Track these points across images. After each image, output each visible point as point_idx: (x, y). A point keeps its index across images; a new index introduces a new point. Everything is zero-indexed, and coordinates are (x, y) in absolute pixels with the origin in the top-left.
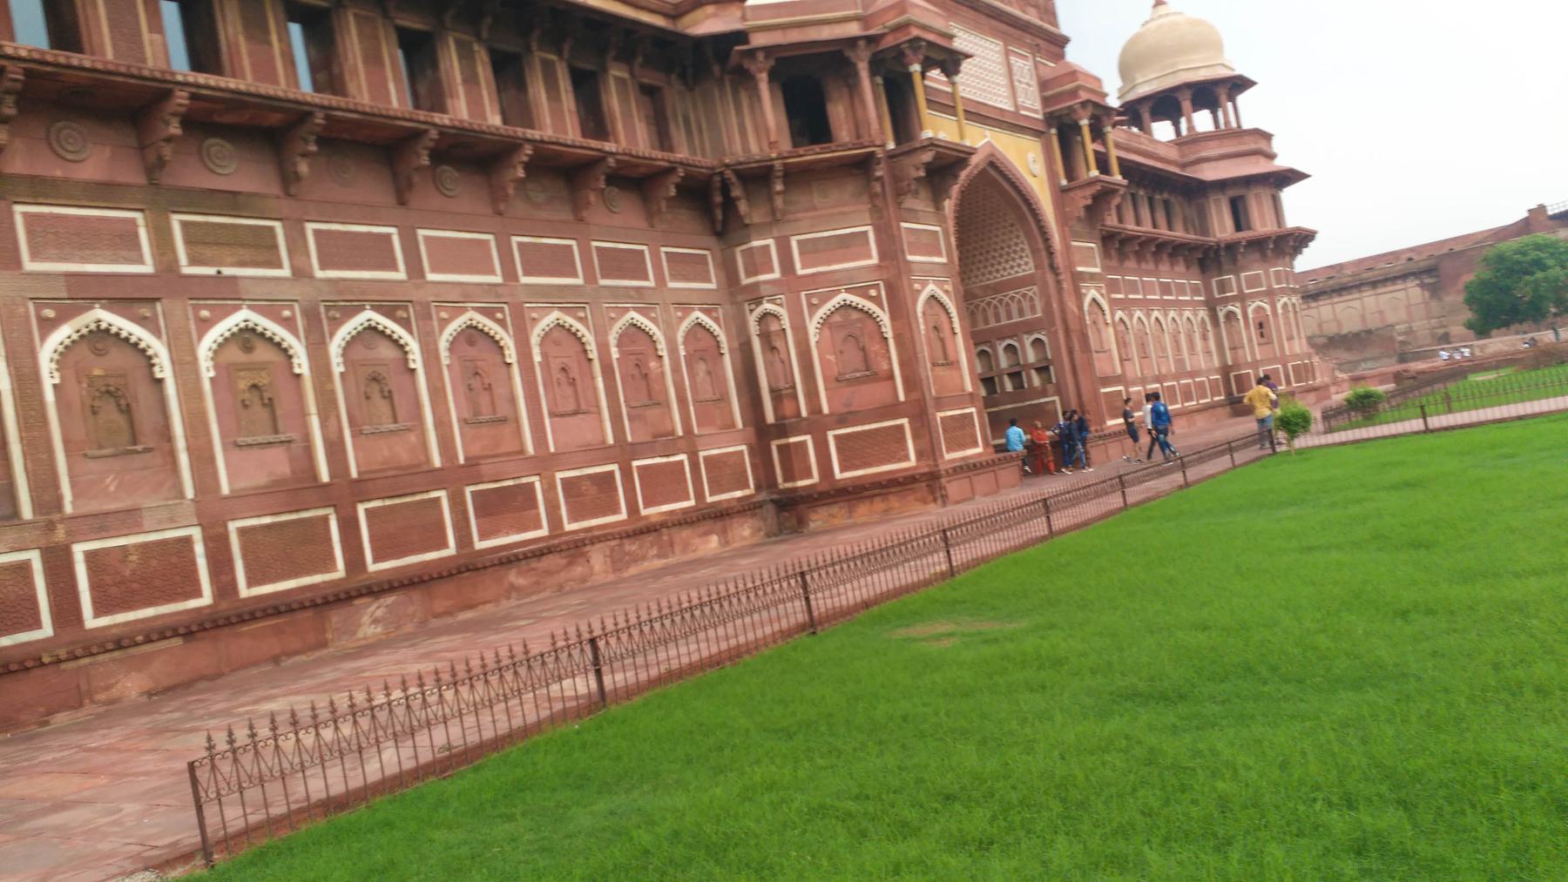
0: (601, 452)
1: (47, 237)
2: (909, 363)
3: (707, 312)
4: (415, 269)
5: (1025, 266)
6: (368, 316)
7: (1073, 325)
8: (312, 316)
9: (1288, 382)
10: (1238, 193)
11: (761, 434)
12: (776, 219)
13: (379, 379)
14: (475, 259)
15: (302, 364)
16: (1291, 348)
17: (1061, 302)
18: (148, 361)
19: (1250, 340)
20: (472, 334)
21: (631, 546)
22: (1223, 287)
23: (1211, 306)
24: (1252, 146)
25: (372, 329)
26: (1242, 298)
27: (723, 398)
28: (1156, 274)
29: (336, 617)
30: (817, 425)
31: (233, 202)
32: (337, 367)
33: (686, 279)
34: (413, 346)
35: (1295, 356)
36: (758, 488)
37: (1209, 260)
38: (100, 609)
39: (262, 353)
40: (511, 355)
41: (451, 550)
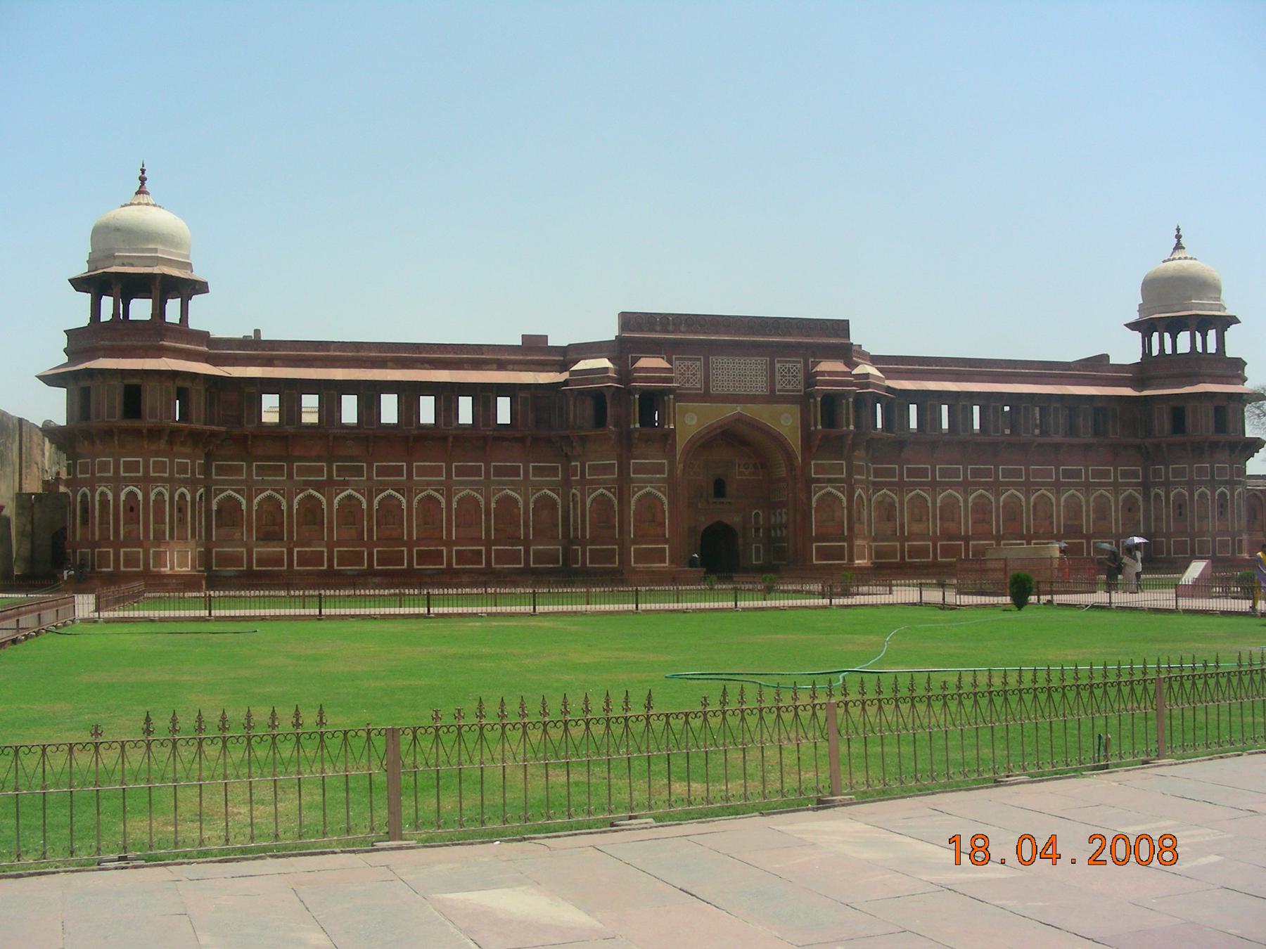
0: (477, 541)
3: (553, 490)
5: (782, 472)
8: (370, 491)
11: (568, 542)
13: (389, 512)
14: (437, 472)
15: (365, 506)
19: (1168, 516)
20: (429, 497)
21: (483, 579)
22: (1157, 473)
23: (1146, 487)
25: (390, 496)
30: (583, 543)
31: (352, 459)
32: (376, 506)
34: (404, 501)
40: (443, 505)
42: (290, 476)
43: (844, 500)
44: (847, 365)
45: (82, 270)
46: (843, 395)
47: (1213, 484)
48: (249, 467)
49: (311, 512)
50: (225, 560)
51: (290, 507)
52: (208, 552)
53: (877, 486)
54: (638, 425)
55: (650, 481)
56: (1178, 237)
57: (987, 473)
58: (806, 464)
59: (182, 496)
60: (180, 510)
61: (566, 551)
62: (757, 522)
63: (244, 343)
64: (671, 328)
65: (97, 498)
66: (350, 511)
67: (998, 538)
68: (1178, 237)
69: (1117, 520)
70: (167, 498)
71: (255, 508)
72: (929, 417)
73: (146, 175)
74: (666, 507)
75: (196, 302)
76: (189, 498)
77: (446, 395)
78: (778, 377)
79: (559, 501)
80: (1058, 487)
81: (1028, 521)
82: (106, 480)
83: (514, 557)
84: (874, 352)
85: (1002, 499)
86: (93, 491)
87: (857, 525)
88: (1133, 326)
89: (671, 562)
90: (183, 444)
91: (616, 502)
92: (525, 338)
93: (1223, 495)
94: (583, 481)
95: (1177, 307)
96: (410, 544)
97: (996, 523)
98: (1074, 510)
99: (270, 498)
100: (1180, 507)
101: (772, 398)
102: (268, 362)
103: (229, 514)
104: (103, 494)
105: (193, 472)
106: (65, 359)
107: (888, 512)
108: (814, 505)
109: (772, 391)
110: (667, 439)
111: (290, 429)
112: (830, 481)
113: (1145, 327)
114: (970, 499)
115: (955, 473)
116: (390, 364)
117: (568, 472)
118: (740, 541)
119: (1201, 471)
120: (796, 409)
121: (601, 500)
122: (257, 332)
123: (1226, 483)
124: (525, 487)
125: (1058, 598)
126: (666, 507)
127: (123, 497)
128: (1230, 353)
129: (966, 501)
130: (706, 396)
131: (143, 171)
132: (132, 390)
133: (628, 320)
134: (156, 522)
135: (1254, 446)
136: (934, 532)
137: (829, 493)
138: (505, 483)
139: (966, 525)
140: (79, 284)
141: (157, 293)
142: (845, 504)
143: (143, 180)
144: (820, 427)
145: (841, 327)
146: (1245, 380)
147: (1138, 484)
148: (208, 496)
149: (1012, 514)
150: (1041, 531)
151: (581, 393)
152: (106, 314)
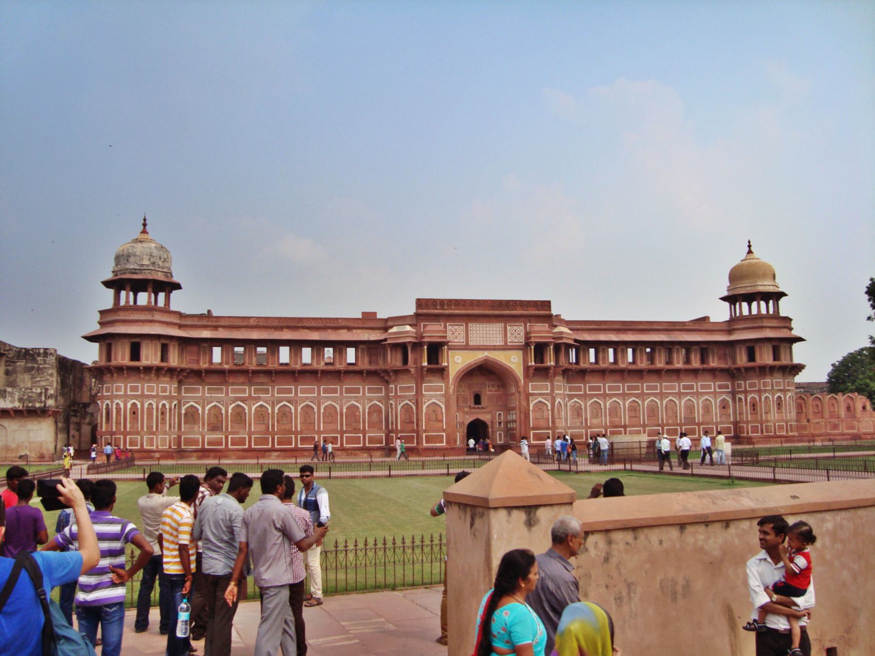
0: (337, 432)
1: (234, 391)
2: (417, 420)
4: (296, 394)
6: (285, 403)
7: (523, 410)
8: (273, 403)
9: (762, 432)
10: (751, 347)
11: (389, 432)
12: (394, 381)
13: (284, 414)
15: (270, 411)
16: (766, 417)
17: (520, 402)
18: (244, 409)
20: (308, 406)
21: (339, 453)
22: (739, 386)
23: (733, 394)
24: (760, 325)
25: (285, 405)
26: (746, 392)
28: (679, 380)
29: (268, 454)
31: (263, 384)
35: (767, 421)
36: (387, 444)
37: (733, 374)
38: (232, 445)
39: (264, 409)
40: (316, 410)
41: (293, 446)
42: (227, 394)
44: (549, 327)
45: (109, 276)
46: (546, 345)
47: (773, 391)
48: (204, 389)
49: (239, 416)
50: (189, 442)
51: (227, 412)
52: (179, 437)
53: (571, 397)
54: (425, 364)
55: (435, 396)
56: (749, 246)
57: (637, 388)
58: (526, 385)
59: (164, 405)
60: (162, 413)
61: (387, 437)
62: (499, 418)
63: (201, 316)
64: (446, 307)
65: (114, 406)
66: (262, 414)
67: (644, 426)
68: (749, 246)
69: (716, 414)
70: (154, 406)
71: (207, 412)
72: (601, 355)
73: (147, 222)
74: (444, 411)
75: (175, 294)
76: (167, 406)
77: (317, 346)
78: (509, 334)
80: (680, 395)
81: (662, 416)
82: (119, 397)
83: (357, 440)
84: (566, 319)
85: (646, 403)
86: (112, 402)
87: (557, 421)
88: (724, 299)
89: (447, 443)
90: (164, 375)
91: (414, 408)
92: (363, 313)
93: (779, 397)
94: (396, 396)
95: (749, 288)
96: (296, 433)
97: (643, 417)
98: (690, 408)
99: (215, 406)
100: (754, 405)
101: (505, 348)
102: (216, 328)
103: (192, 416)
104: (117, 404)
105: (170, 392)
106: (98, 327)
107: (578, 412)
108: (531, 408)
109: (506, 343)
110: (442, 372)
111: (226, 367)
112: (540, 394)
113: (732, 299)
114: (627, 403)
115: (618, 388)
116: (285, 330)
117: (387, 390)
118: (490, 430)
119: (765, 385)
120: (520, 353)
121: (407, 408)
122: (209, 311)
123: (780, 390)
124: (364, 398)
125: (636, 467)
126: (444, 411)
127: (129, 406)
128: (783, 313)
129: (624, 405)
130: (467, 347)
131: (145, 220)
132: (135, 345)
133: (420, 303)
134: (148, 419)
135: (799, 368)
136: (606, 423)
137: (540, 402)
138: (352, 397)
139: (625, 418)
140: (108, 284)
141: (150, 289)
142: (550, 408)
143: (145, 225)
144: (533, 363)
145: (547, 305)
146: (791, 329)
147: (728, 392)
148: (179, 405)
149: (653, 411)
150: (670, 422)
151: (395, 346)
152: (123, 302)
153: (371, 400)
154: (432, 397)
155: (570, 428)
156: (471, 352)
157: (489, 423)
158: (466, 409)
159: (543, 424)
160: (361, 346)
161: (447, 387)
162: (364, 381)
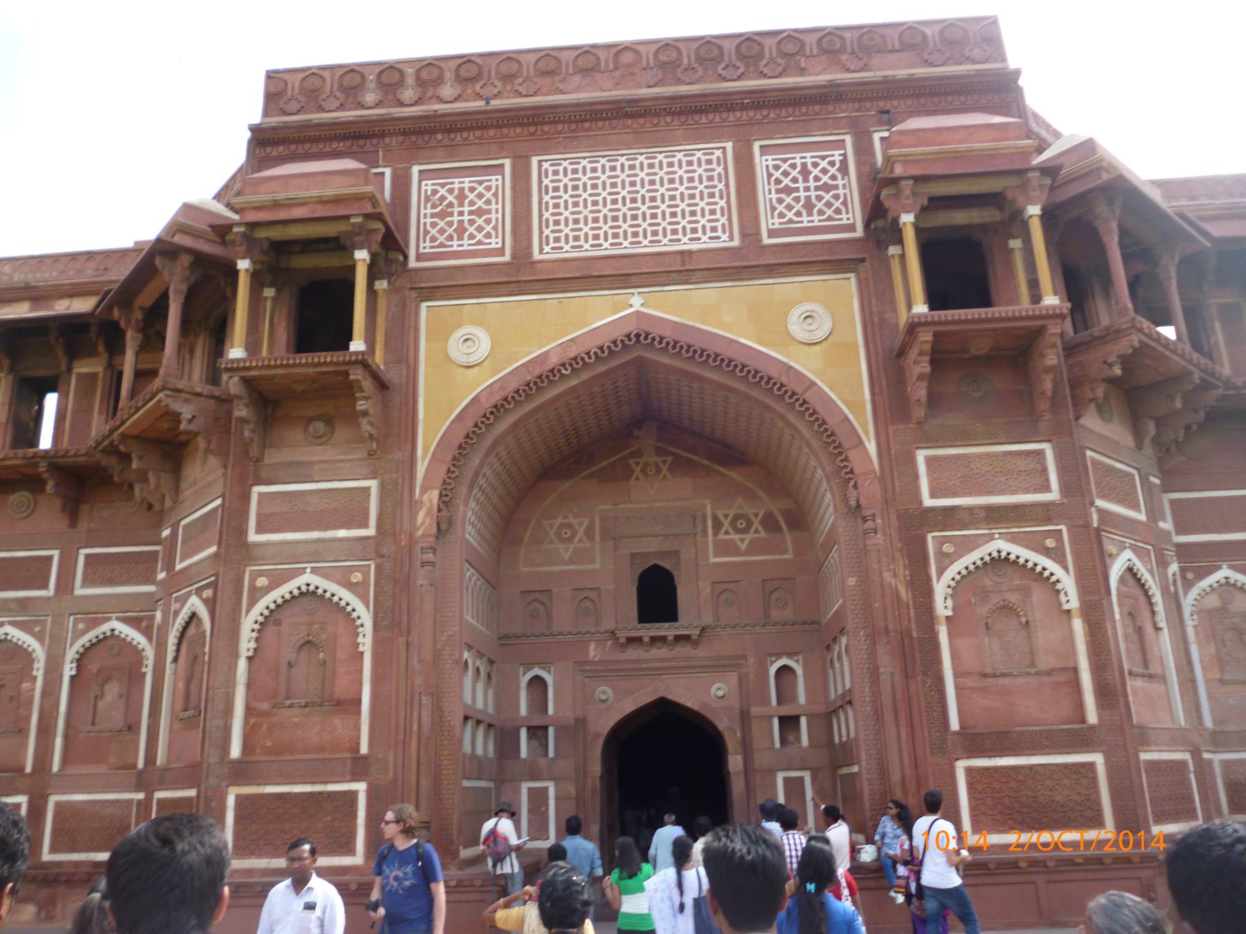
3: (133, 622)
27: (132, 728)
33: (111, 582)
43: (1068, 583)
55: (313, 553)
58: (897, 464)
64: (408, 94)
78: (765, 193)
79: (150, 653)
91: (208, 633)
101: (749, 262)
108: (943, 606)
109: (750, 231)
112: (995, 516)
118: (735, 762)
120: (847, 286)
126: (366, 643)
130: (520, 276)
137: (1000, 562)
144: (921, 308)
153: (93, 614)
154: (298, 555)
155: (1219, 740)
156: (552, 300)
157: (722, 724)
158: (593, 652)
159: (1033, 707)
160: (83, 368)
161: (397, 497)
162: (74, 519)
